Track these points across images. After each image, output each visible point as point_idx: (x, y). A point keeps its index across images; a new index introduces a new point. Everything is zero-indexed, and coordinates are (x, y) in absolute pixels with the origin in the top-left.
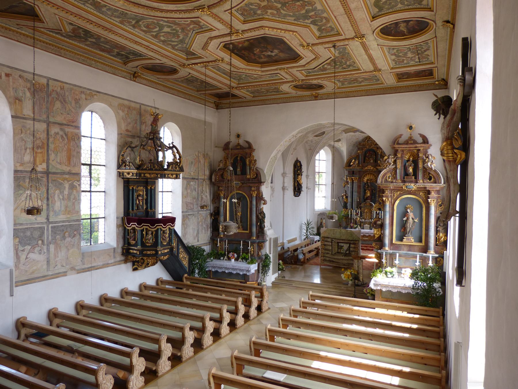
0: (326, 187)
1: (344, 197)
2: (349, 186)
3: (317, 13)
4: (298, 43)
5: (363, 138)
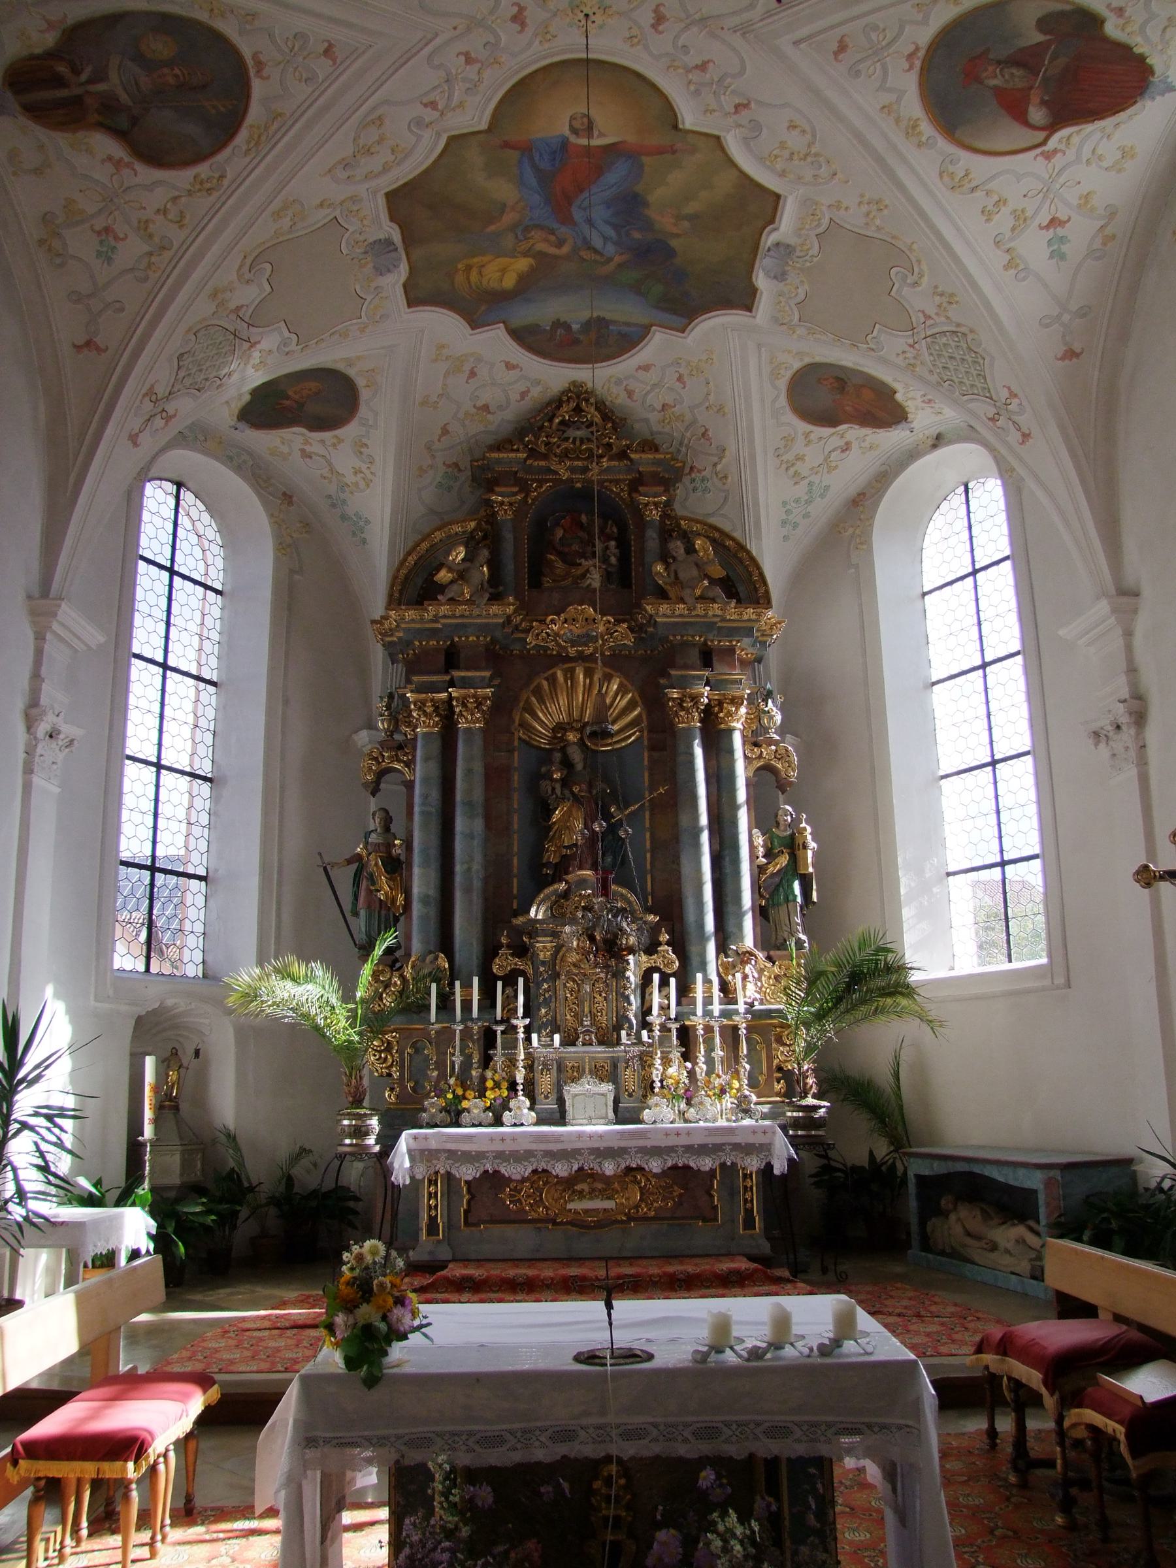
0: (215, 798)
1: (375, 864)
2: (419, 773)
5: (527, 403)
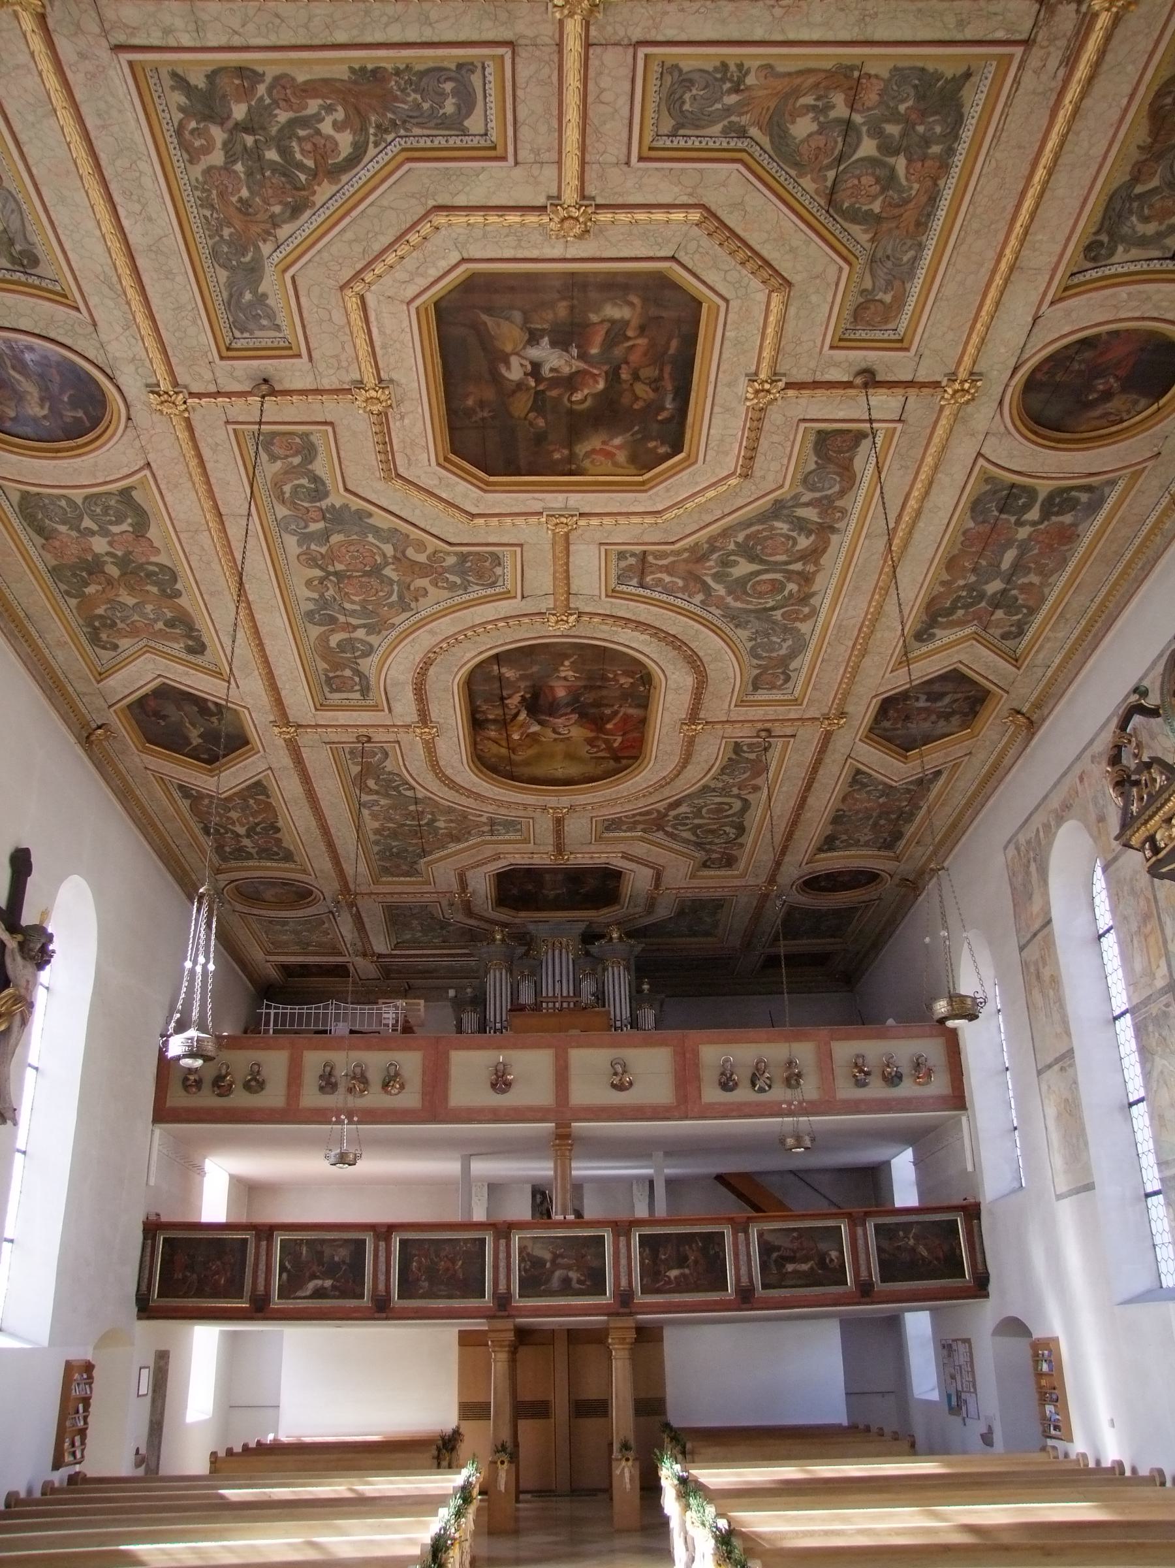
3: (302, 524)
4: (402, 418)
